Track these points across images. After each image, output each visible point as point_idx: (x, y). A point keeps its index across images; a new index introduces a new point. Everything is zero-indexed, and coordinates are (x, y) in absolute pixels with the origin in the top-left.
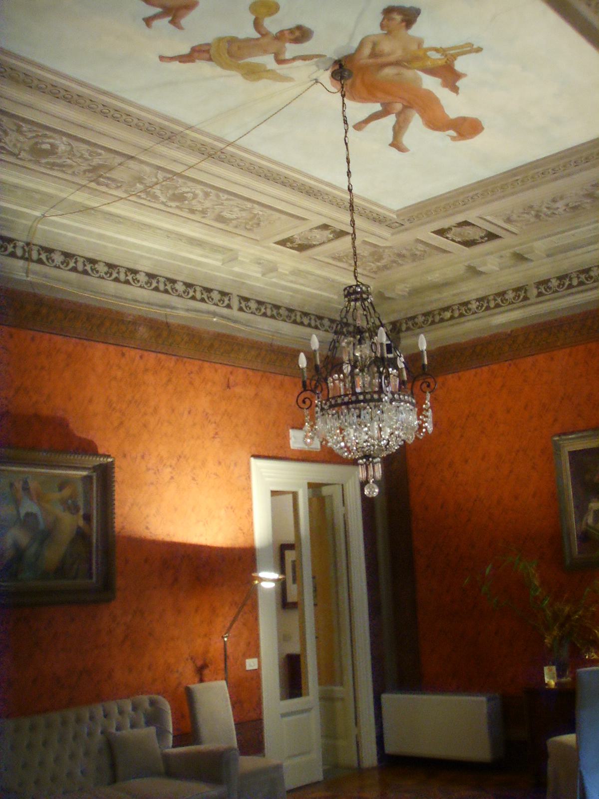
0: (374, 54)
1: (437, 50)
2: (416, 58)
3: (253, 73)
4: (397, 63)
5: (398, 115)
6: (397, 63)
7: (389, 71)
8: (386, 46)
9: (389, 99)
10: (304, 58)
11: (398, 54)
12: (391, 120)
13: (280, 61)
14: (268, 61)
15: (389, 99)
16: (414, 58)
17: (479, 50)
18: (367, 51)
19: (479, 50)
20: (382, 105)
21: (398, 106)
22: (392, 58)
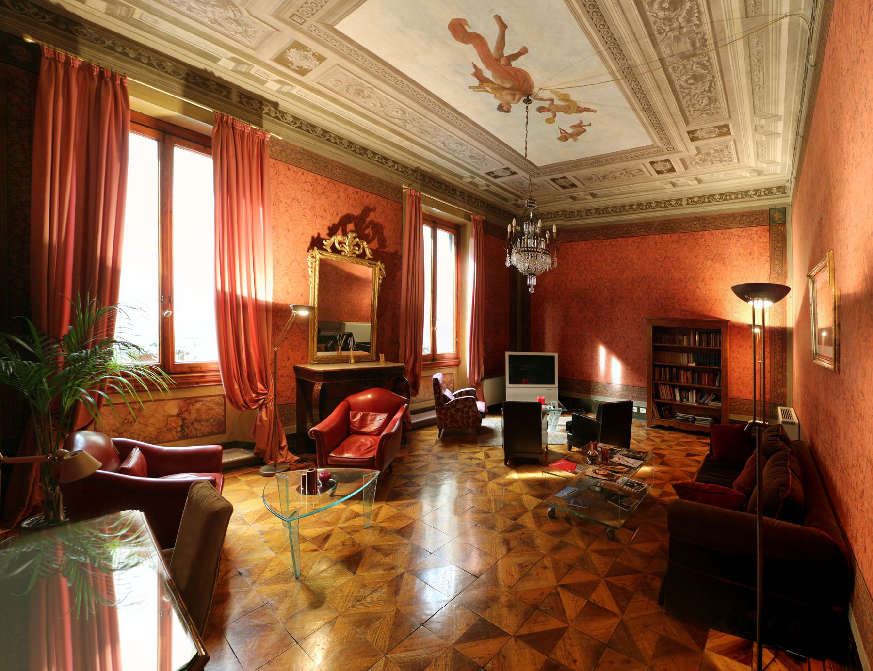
0: (514, 95)
1: (488, 91)
2: (496, 89)
3: (565, 98)
4: (505, 89)
5: (502, 55)
6: (505, 89)
7: (508, 86)
8: (509, 98)
9: (507, 68)
10: (542, 100)
11: (504, 93)
12: (508, 51)
13: (552, 100)
14: (557, 102)
15: (507, 68)
16: (498, 89)
17: (470, 87)
18: (517, 97)
19: (470, 87)
20: (510, 65)
21: (503, 61)
22: (507, 91)
